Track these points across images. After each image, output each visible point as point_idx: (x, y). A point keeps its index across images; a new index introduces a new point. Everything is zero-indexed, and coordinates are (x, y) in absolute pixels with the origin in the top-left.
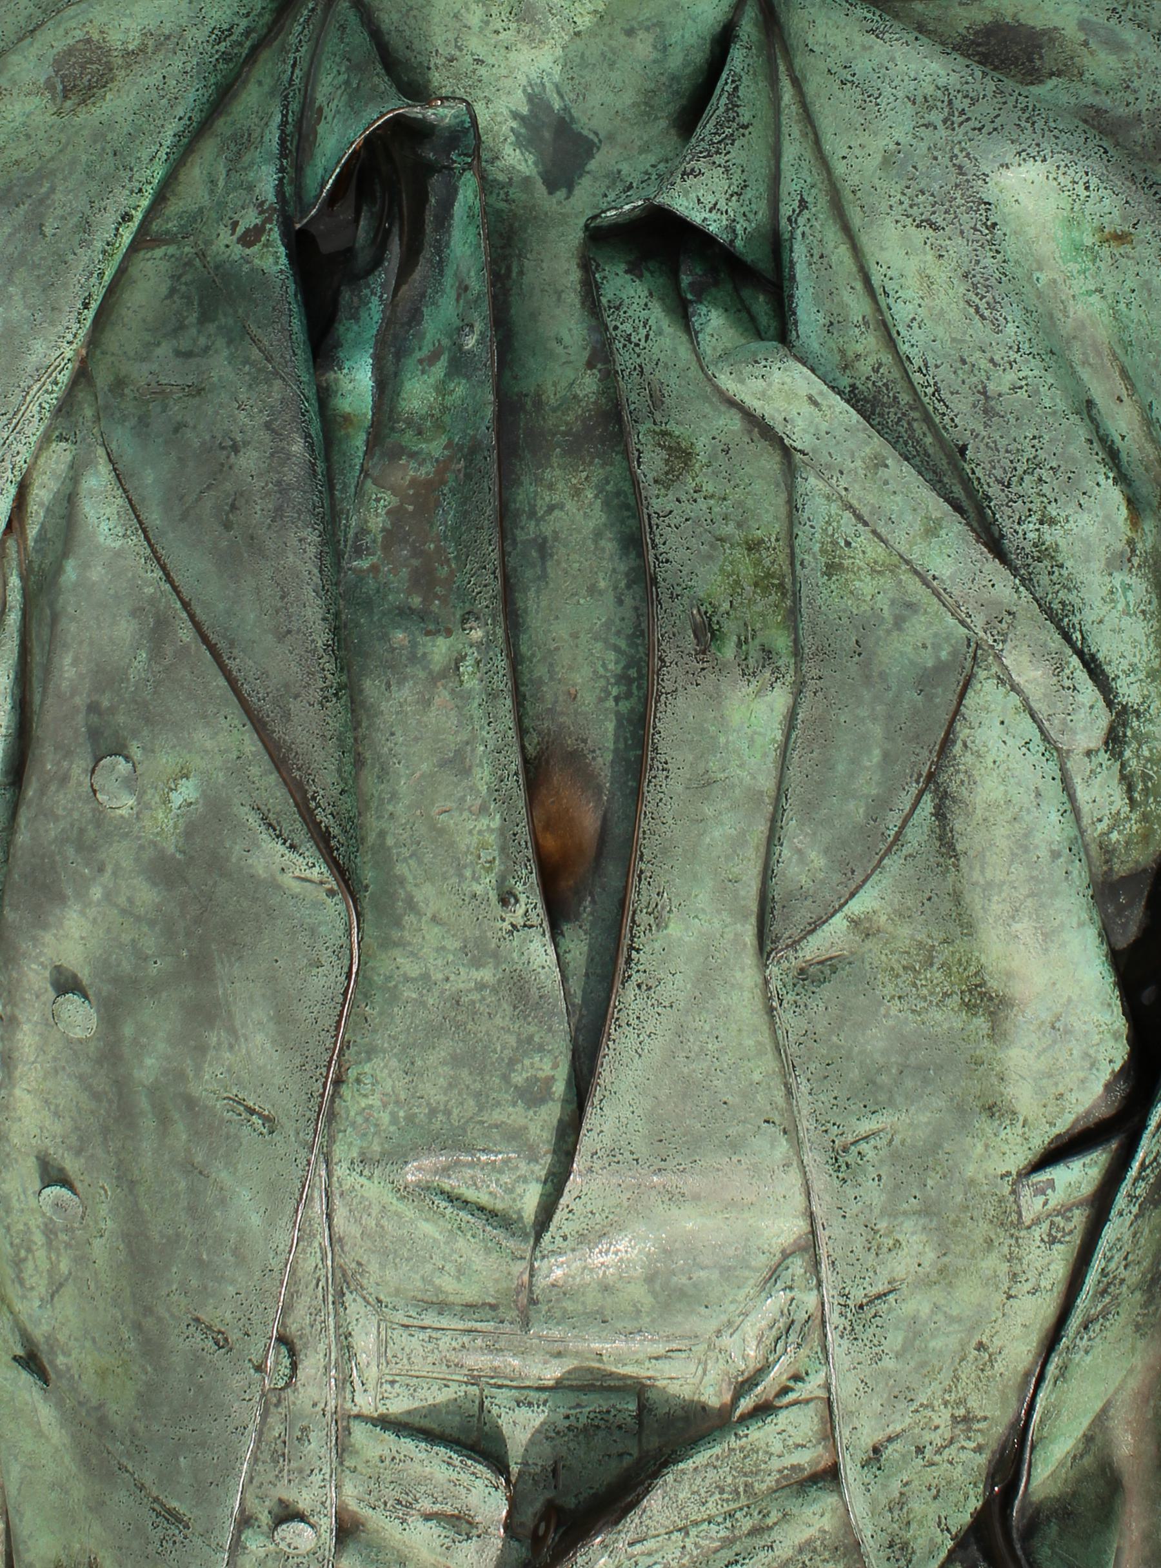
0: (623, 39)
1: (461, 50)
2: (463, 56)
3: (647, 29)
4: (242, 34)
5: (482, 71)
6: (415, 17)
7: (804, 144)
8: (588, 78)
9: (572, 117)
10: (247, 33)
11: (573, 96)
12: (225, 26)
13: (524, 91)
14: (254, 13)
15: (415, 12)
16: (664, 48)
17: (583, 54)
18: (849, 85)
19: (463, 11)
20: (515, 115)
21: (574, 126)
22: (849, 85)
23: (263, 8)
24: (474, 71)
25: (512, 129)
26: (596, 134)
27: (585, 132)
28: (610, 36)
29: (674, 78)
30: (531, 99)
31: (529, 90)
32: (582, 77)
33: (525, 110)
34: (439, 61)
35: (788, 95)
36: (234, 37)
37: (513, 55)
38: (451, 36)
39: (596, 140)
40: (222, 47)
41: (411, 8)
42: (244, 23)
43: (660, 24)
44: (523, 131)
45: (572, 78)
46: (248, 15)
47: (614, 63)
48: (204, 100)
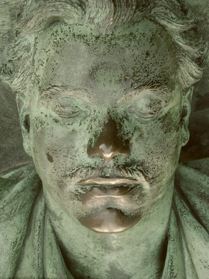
0: (137, 247)
1: (88, 254)
2: (89, 256)
3: (143, 242)
4: (20, 240)
5: (95, 261)
6: (73, 242)
7: (193, 277)
8: (127, 260)
9: (124, 271)
10: (21, 238)
11: (123, 265)
12: (15, 240)
13: (109, 265)
14: (22, 229)
15: (72, 240)
16: (149, 246)
17: (125, 254)
18: (207, 269)
19: (87, 243)
20: (107, 271)
21: (124, 272)
22: (207, 269)
23: (24, 226)
24: (93, 260)
25: (106, 275)
26: (131, 274)
27: (127, 274)
28: (133, 248)
29: (153, 252)
30: (111, 267)
31: (110, 265)
32: (126, 260)
33: (109, 270)
34: (82, 256)
35: (187, 258)
36: (18, 243)
37: (104, 257)
38: (85, 250)
39: (131, 275)
40: (15, 249)
41: (71, 239)
42: (19, 236)
43: (147, 240)
44: (109, 275)
45: (123, 261)
46: (20, 232)
47: (135, 255)
48: (13, 270)
